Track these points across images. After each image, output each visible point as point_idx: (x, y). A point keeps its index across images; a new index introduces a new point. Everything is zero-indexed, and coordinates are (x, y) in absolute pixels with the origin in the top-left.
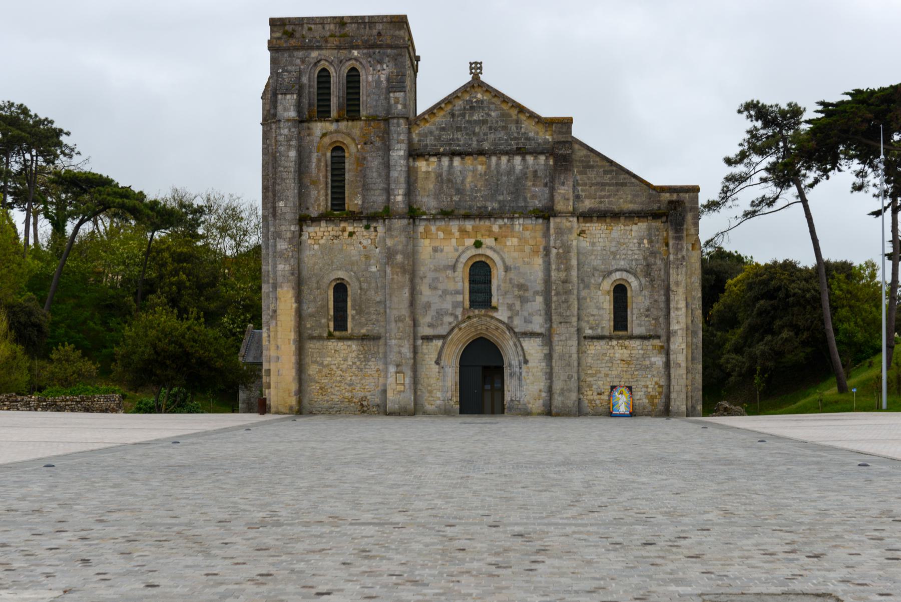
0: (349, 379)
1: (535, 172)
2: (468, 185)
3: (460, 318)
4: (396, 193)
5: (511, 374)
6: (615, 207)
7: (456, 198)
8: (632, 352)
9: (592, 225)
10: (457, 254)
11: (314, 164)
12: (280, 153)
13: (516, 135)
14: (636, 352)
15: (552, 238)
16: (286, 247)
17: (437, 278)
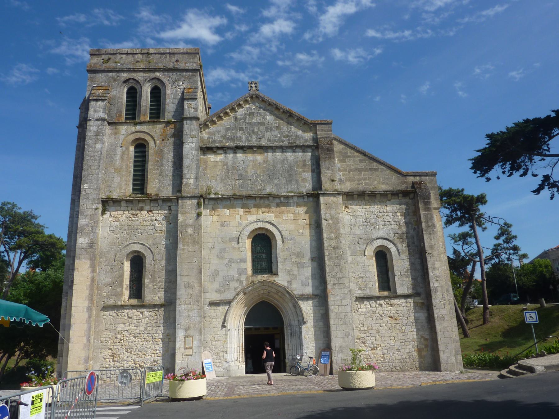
0: (141, 343)
1: (304, 161)
2: (249, 172)
3: (244, 284)
4: (188, 176)
5: (291, 334)
6: (370, 187)
7: (240, 182)
8: (398, 309)
9: (354, 202)
10: (241, 228)
11: (119, 156)
12: (88, 145)
13: (287, 133)
14: (401, 308)
15: (323, 212)
16: (87, 222)
17: (224, 249)
